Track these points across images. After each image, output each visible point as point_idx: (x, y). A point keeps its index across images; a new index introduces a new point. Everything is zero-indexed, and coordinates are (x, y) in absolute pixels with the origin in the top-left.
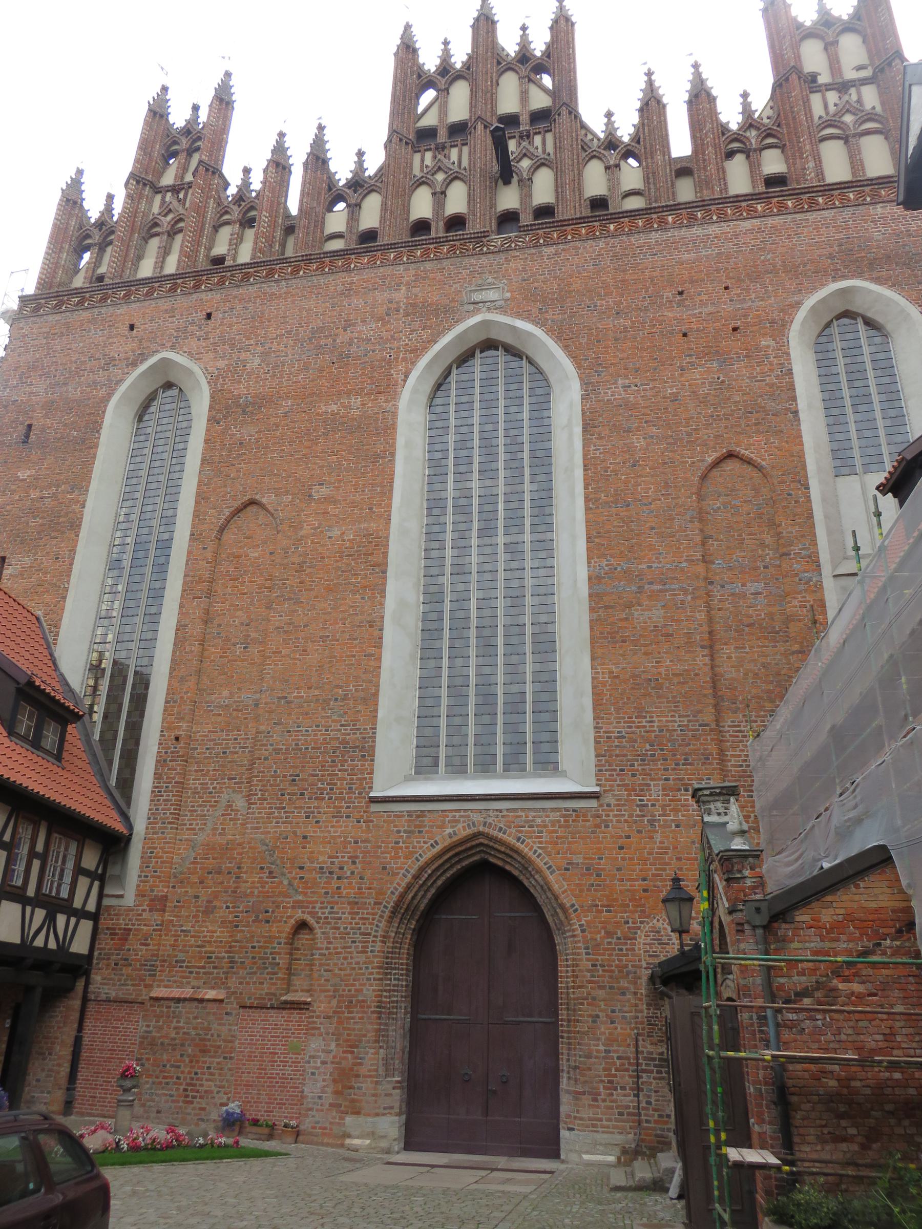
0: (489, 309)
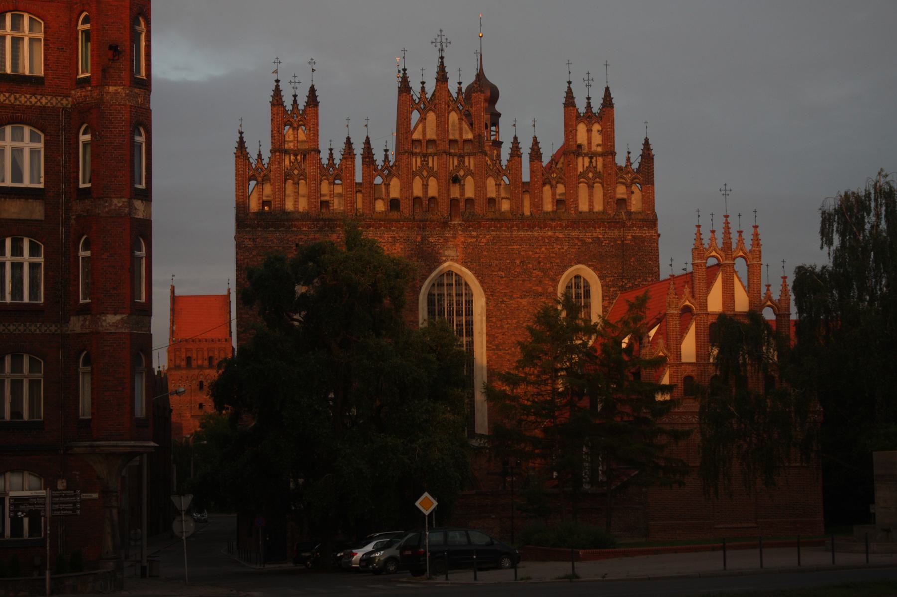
0: (451, 260)
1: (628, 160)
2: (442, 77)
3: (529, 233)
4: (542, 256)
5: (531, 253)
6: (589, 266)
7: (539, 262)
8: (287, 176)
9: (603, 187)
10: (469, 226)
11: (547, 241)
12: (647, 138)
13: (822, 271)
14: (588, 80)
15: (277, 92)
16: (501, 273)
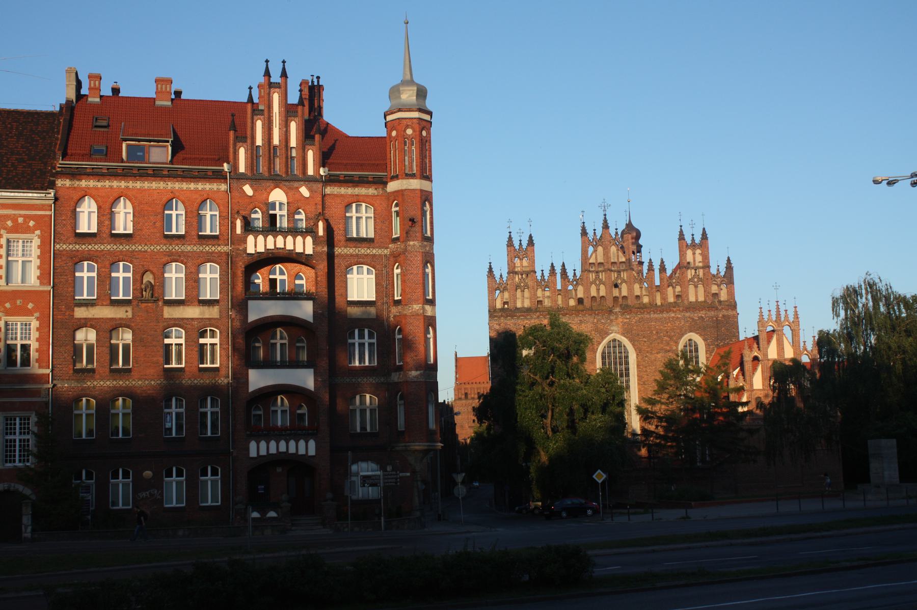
0: (615, 332)
1: (718, 270)
2: (606, 226)
3: (660, 315)
4: (669, 328)
5: (662, 327)
6: (697, 333)
7: (667, 332)
8: (517, 287)
9: (704, 286)
10: (625, 312)
11: (671, 319)
13: (833, 332)
14: (692, 224)
15: (510, 238)
16: (644, 339)
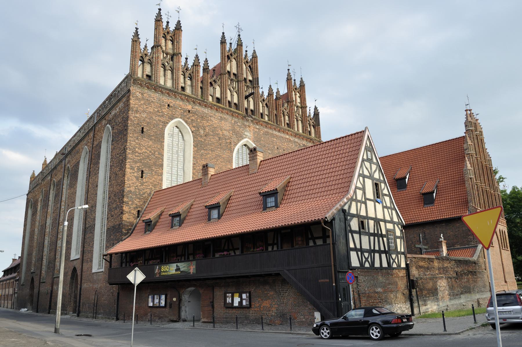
5: (281, 144)
12: (315, 106)
15: (159, 15)
16: (269, 151)
